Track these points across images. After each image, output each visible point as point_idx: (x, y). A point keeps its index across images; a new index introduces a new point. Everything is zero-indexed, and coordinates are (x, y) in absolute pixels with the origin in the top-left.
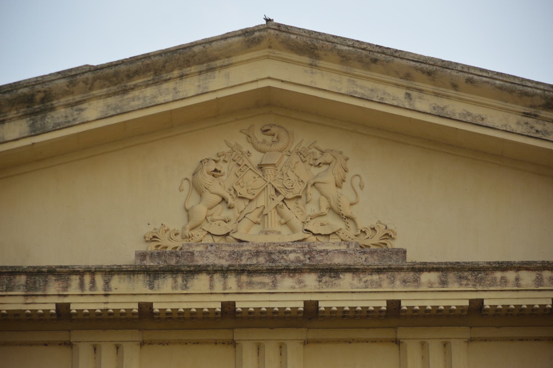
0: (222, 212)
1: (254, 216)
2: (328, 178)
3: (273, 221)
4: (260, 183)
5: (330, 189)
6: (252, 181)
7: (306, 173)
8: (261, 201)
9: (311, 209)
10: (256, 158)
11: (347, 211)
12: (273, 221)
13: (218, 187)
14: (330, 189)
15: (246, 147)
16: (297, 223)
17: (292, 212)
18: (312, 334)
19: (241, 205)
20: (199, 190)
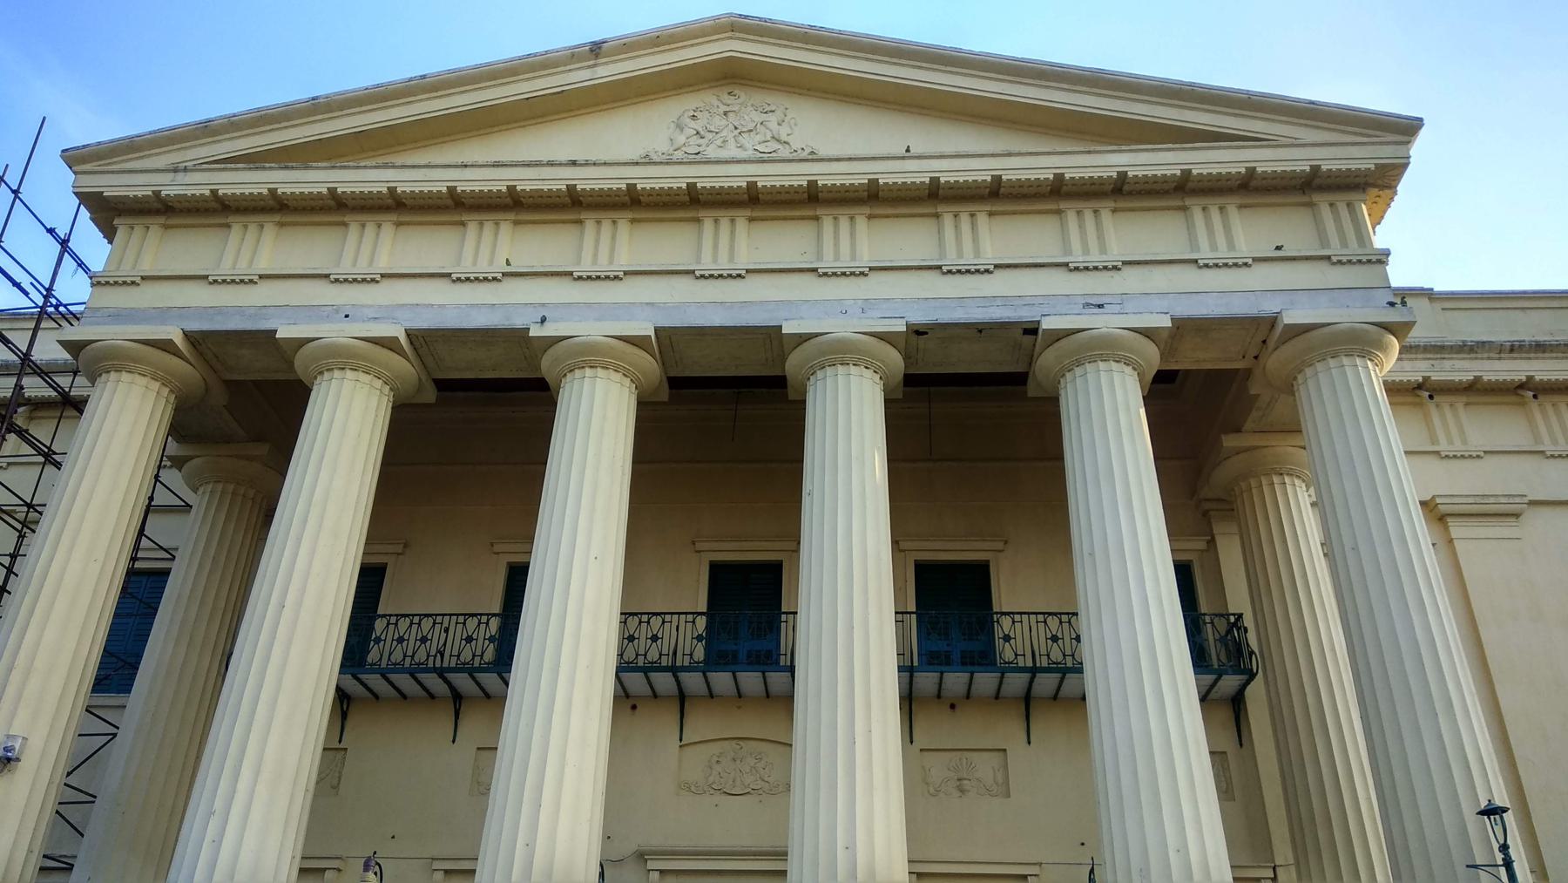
0: (695, 140)
1: (719, 142)
2: (772, 120)
3: (732, 143)
4: (724, 122)
5: (773, 125)
6: (719, 122)
7: (758, 117)
8: (724, 134)
9: (759, 138)
10: (723, 108)
11: (784, 138)
12: (732, 143)
13: (692, 124)
14: (773, 125)
15: (716, 103)
16: (748, 146)
17: (746, 140)
18: (755, 214)
19: (710, 136)
20: (680, 127)
